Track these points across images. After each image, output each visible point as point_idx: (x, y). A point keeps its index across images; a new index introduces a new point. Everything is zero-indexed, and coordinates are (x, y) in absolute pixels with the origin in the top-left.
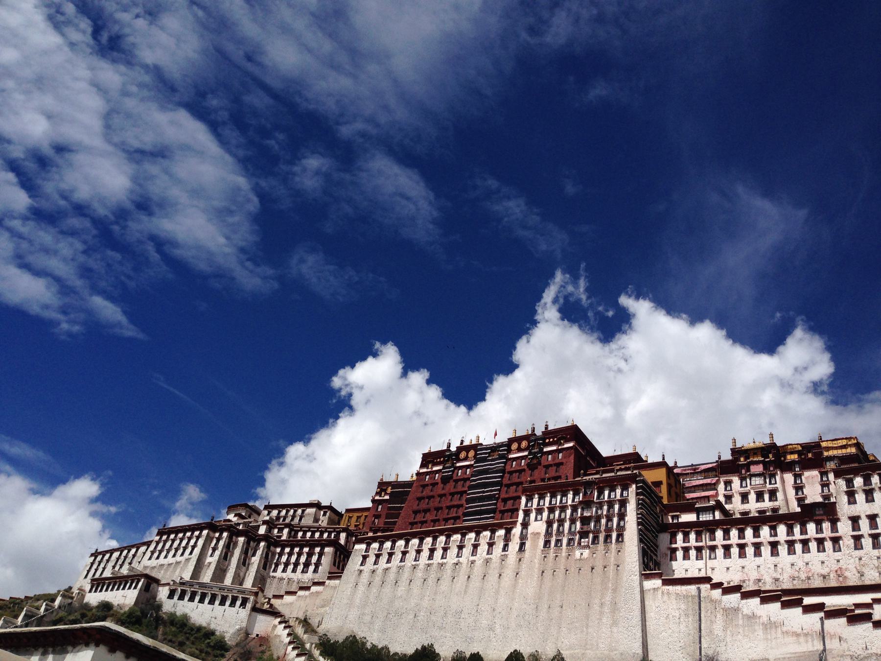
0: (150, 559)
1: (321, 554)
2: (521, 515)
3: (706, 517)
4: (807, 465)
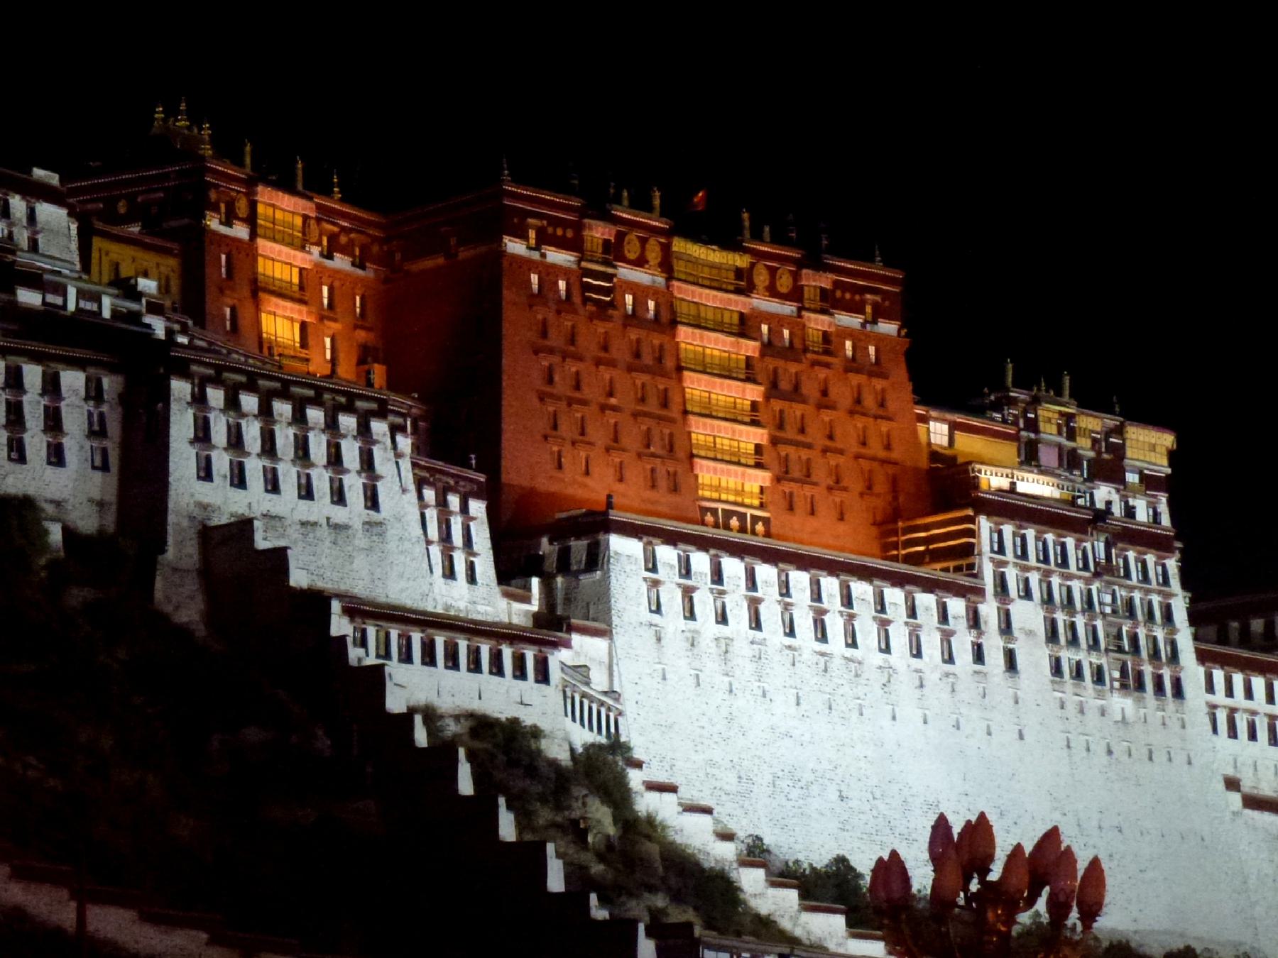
0: (206, 473)
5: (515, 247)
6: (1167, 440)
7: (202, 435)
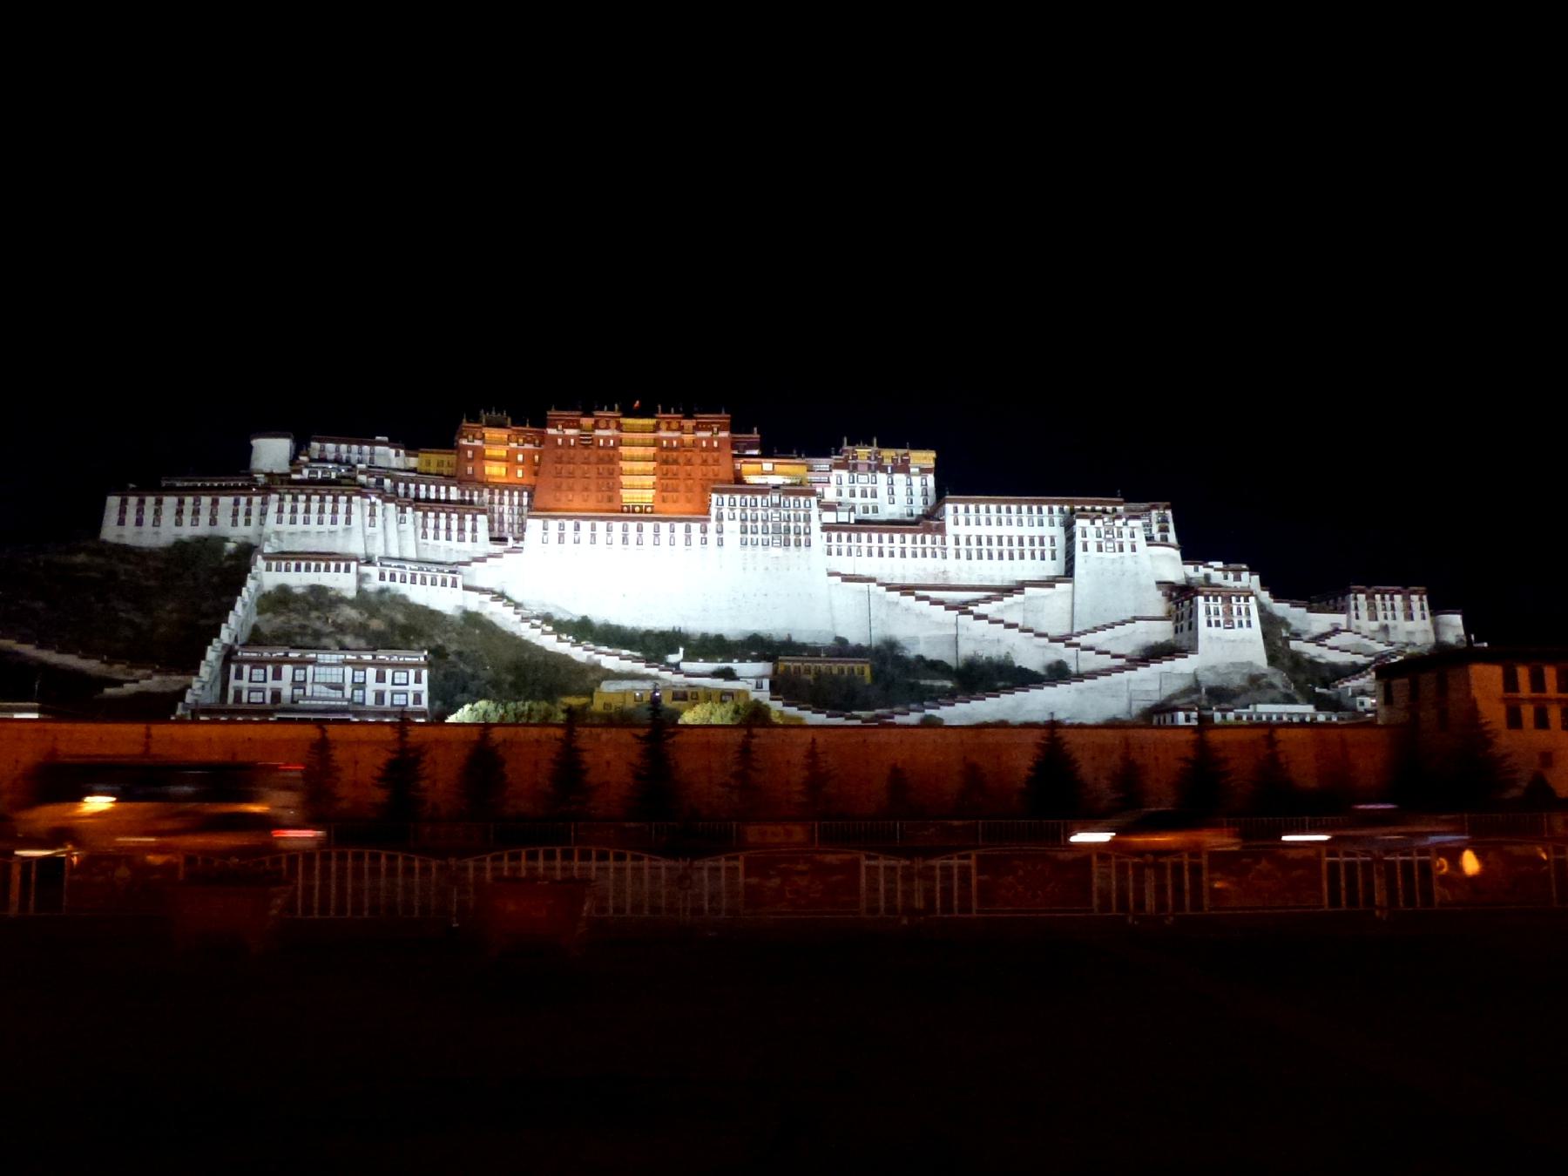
0: (280, 521)
1: (474, 519)
2: (714, 511)
3: (843, 517)
4: (896, 469)
5: (551, 431)
6: (932, 455)
7: (280, 510)
